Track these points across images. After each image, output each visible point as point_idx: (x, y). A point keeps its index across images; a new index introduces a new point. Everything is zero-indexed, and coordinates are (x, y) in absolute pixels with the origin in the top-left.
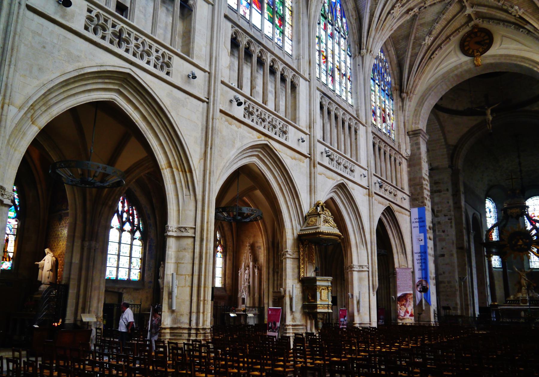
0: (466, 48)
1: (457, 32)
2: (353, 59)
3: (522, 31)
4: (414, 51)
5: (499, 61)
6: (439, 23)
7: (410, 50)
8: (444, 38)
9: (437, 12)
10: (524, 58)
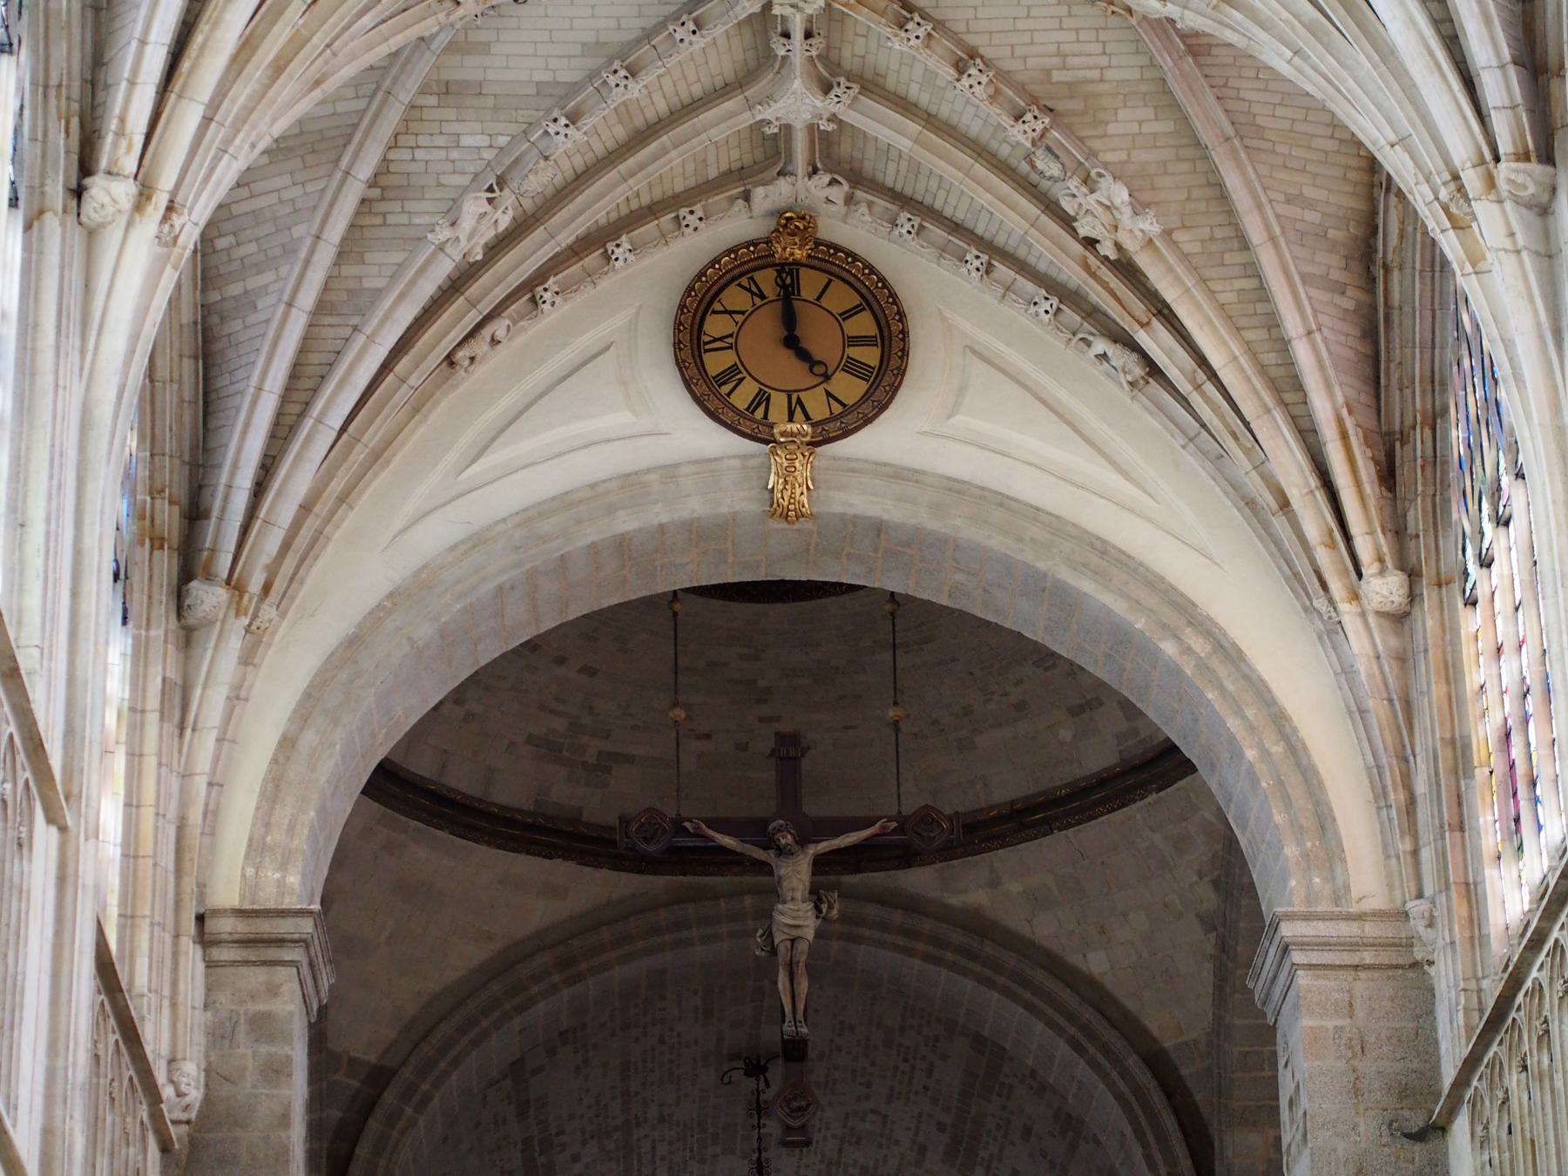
0: (716, 363)
1: (666, 220)
2: (28, 227)
3: (1103, 357)
4: (349, 270)
5: (932, 524)
6: (588, 122)
7: (325, 256)
8: (565, 239)
9: (590, 38)
10: (1102, 547)
